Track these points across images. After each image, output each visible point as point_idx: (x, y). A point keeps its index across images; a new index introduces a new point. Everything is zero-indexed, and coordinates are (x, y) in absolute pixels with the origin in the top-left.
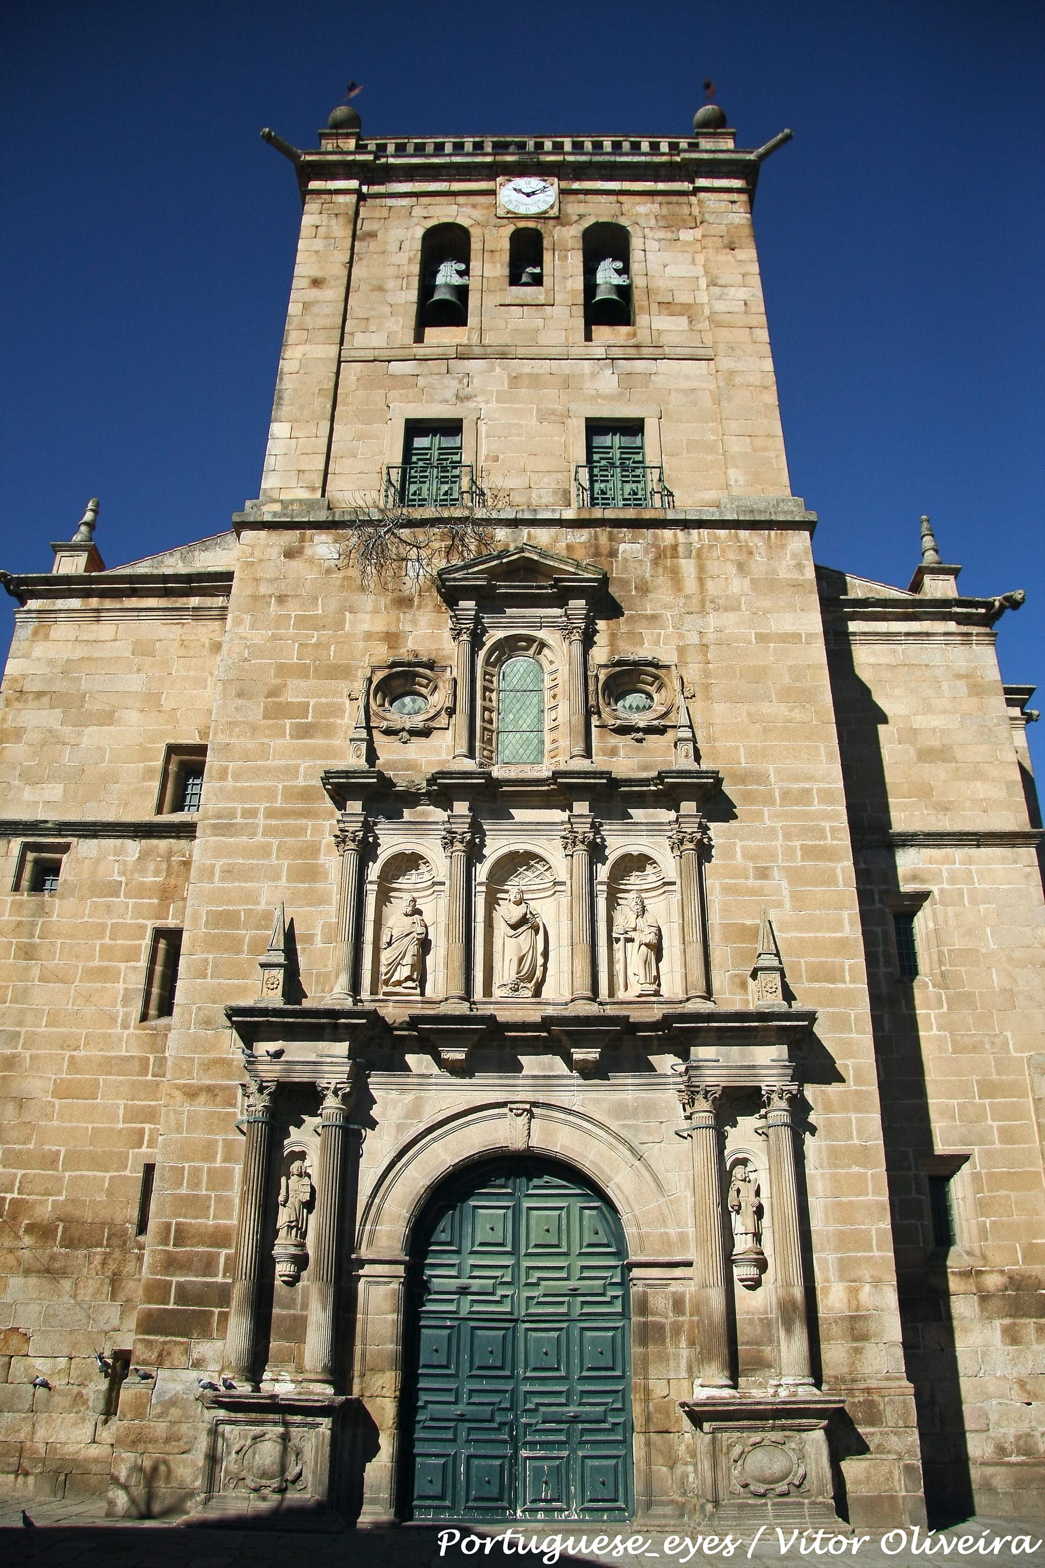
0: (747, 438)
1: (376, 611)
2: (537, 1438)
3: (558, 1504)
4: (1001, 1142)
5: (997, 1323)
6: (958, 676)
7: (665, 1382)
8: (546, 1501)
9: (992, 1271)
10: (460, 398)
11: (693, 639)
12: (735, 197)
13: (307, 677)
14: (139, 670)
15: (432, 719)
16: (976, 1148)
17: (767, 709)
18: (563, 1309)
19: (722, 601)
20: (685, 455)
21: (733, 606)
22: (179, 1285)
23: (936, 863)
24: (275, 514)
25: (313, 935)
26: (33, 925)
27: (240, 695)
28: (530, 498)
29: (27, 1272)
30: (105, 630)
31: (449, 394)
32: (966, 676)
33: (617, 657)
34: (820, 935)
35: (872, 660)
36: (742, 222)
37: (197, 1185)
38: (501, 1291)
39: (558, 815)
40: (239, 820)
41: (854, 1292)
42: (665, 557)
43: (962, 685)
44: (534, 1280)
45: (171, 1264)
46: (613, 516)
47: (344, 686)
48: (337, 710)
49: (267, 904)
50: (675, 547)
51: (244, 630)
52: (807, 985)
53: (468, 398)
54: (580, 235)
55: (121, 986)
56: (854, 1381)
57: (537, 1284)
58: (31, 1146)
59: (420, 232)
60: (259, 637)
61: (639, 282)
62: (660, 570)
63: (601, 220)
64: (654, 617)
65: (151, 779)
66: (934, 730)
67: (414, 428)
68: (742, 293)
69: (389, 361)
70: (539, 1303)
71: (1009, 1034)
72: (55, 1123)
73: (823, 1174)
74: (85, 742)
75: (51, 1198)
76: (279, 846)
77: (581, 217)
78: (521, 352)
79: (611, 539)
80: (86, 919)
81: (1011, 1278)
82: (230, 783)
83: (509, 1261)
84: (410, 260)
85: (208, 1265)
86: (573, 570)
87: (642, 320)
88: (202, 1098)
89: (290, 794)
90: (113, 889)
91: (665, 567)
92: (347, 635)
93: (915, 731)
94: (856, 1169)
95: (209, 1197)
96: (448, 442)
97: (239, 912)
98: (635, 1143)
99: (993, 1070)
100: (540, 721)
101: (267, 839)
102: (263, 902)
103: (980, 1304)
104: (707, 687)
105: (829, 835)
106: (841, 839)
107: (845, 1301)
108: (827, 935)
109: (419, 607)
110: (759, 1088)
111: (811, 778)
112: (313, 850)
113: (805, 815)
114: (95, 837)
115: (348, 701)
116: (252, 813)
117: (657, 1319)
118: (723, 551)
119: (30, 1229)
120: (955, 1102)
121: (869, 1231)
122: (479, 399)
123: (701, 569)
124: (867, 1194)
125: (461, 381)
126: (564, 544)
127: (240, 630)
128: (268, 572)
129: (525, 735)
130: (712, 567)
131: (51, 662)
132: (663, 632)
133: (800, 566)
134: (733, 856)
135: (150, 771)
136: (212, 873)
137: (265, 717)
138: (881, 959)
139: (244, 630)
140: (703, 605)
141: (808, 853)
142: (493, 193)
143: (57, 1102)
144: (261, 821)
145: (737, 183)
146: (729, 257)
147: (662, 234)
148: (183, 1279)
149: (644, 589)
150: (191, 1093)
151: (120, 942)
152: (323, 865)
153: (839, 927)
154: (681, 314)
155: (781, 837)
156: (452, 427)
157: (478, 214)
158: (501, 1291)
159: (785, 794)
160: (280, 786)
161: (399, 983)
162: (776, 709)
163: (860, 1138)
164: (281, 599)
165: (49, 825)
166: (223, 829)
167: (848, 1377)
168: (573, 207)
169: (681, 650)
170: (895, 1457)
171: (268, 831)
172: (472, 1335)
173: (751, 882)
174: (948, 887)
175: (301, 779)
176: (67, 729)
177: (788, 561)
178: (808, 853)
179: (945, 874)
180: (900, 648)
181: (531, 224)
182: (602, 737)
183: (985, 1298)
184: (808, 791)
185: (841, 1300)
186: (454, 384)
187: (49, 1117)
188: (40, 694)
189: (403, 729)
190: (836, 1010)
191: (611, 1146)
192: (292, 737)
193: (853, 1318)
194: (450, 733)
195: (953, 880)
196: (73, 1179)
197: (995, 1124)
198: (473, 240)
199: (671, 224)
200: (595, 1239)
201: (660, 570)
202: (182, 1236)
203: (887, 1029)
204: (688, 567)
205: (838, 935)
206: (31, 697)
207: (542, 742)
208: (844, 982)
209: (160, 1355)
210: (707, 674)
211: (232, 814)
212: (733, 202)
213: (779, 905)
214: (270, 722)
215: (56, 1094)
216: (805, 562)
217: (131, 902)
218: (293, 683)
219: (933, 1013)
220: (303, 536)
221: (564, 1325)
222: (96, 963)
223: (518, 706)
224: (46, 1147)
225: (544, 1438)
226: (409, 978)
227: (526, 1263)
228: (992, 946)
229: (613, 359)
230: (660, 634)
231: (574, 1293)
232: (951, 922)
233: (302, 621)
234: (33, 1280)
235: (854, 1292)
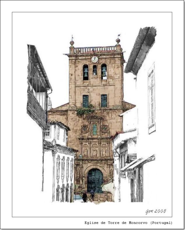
12: (119, 58)
59: (83, 65)
168: (101, 61)
204: (110, 114)
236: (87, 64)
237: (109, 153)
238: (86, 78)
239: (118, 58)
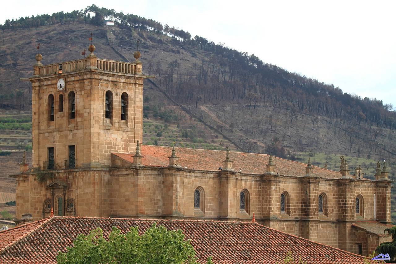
6: (132, 183)
11: (76, 194)
43: (132, 185)
59: (47, 97)
64: (72, 191)
87: (76, 118)
93: (125, 195)
130: (79, 179)
140: (78, 187)
142: (56, 84)
149: (72, 185)
164: (35, 188)
169: (75, 196)
186: (52, 138)
188: (20, 197)
204: (76, 180)
218: (37, 204)
238: (51, 118)
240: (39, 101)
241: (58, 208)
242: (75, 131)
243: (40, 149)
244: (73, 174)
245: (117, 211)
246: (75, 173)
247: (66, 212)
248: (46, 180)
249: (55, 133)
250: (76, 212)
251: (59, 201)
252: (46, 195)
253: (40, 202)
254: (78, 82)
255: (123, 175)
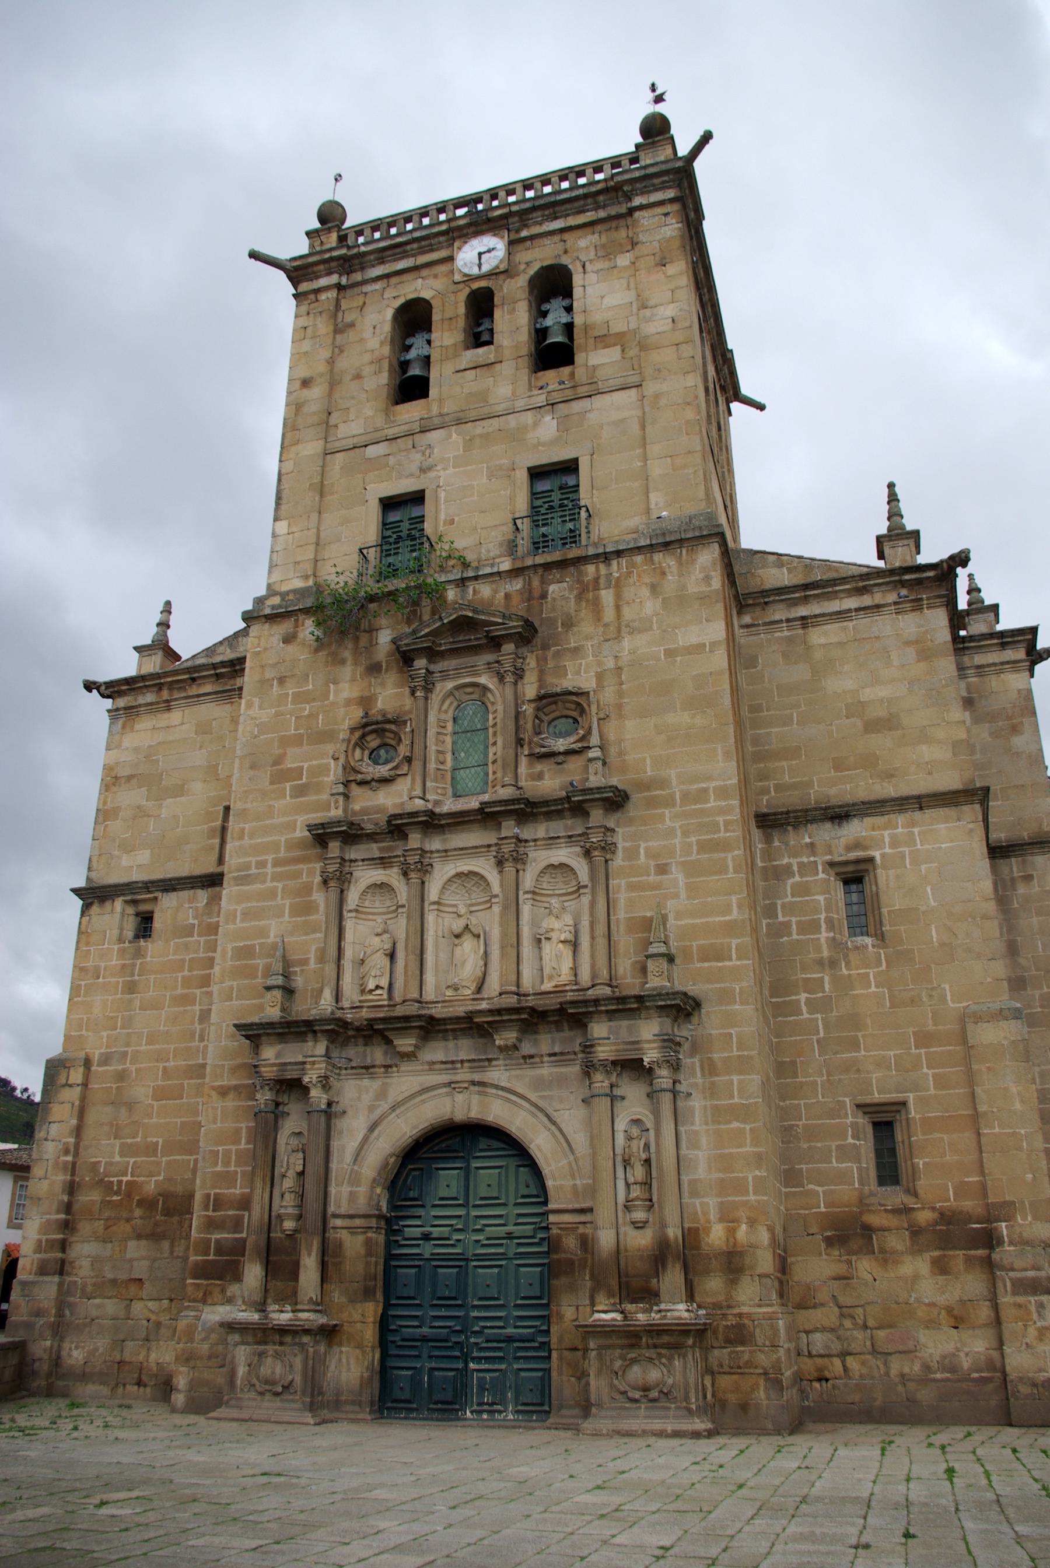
0: (669, 459)
1: (353, 680)
2: (482, 1354)
3: (499, 1407)
4: (935, 1088)
5: (928, 1255)
6: (908, 643)
7: (574, 1308)
8: (487, 1404)
9: (923, 1208)
10: (423, 470)
11: (610, 663)
12: (668, 208)
13: (301, 744)
14: (201, 747)
15: (395, 768)
16: (911, 1096)
17: (671, 719)
18: (501, 1250)
19: (636, 624)
20: (614, 487)
21: (644, 626)
22: (217, 1241)
23: (879, 828)
24: (273, 607)
25: (308, 959)
26: (134, 965)
27: (253, 767)
28: (480, 553)
29: (139, 1237)
30: (175, 716)
31: (414, 468)
32: (917, 642)
33: (542, 692)
34: (710, 919)
35: (823, 640)
36: (674, 234)
37: (227, 1163)
38: (455, 1237)
39: (490, 838)
40: (253, 871)
41: (731, 1232)
42: (588, 591)
43: (911, 652)
44: (478, 1227)
45: (211, 1225)
46: (542, 562)
47: (330, 748)
48: (324, 770)
49: (275, 937)
50: (596, 580)
51: (255, 711)
52: (698, 965)
53: (430, 469)
54: (526, 284)
55: (197, 1008)
56: (729, 1307)
57: (481, 1230)
58: (139, 1140)
59: (389, 314)
60: (265, 715)
61: (578, 320)
62: (584, 604)
63: (545, 264)
65: (213, 837)
66: (882, 701)
67: (389, 504)
68: (670, 311)
69: (366, 446)
70: (484, 1245)
71: (947, 987)
72: (155, 1120)
73: (707, 1131)
74: (164, 813)
75: (154, 1179)
76: (283, 889)
77: (528, 264)
78: (473, 414)
79: (543, 582)
80: (170, 957)
81: (942, 1214)
82: (246, 841)
83: (461, 1212)
84: (382, 343)
85: (237, 1225)
86: (500, 621)
87: (579, 358)
88: (231, 1095)
89: (291, 845)
90: (189, 931)
91: (587, 601)
92: (332, 704)
93: (863, 704)
94: (735, 1125)
95: (236, 1172)
96: (415, 512)
97: (254, 945)
98: (550, 1111)
99: (930, 1022)
100: (486, 755)
101: (275, 884)
102: (272, 935)
103: (911, 1238)
104: (620, 706)
105: (722, 828)
106: (733, 831)
107: (724, 1238)
108: (717, 919)
109: (387, 670)
110: (642, 1060)
111: (709, 778)
112: (307, 889)
113: (702, 812)
114: (174, 890)
115: (332, 761)
116: (262, 864)
117: (569, 1256)
118: (639, 576)
119: (140, 1203)
120: (892, 1053)
121: (746, 1179)
122: (438, 468)
123: (618, 596)
124: (746, 1146)
125: (424, 454)
126: (502, 594)
127: (251, 712)
128: (271, 658)
129: (473, 770)
130: (628, 593)
131: (136, 750)
132: (583, 662)
133: (707, 579)
134: (637, 857)
135: (212, 830)
136: (235, 917)
137: (272, 783)
138: (824, 926)
139: (255, 711)
140: (618, 631)
141: (704, 847)
142: (451, 259)
143: (155, 1103)
144: (269, 869)
145: (671, 194)
146: (661, 276)
147: (600, 265)
148: (218, 1236)
149: (569, 624)
150: (223, 1092)
151: (195, 973)
152: (315, 901)
153: (728, 910)
154: (614, 345)
155: (679, 833)
156: (417, 498)
157: (439, 284)
158: (455, 1237)
159: (685, 796)
160: (283, 840)
161: (371, 991)
162: (680, 718)
163: (741, 1097)
164: (282, 680)
165: (140, 885)
166: (243, 880)
167: (725, 1304)
168: (523, 256)
169: (600, 677)
170: (761, 1371)
171: (276, 877)
172: (517, 1272)
173: (652, 878)
174: (891, 851)
175: (298, 831)
176: (150, 803)
177: (697, 574)
178: (704, 847)
179: (887, 840)
180: (850, 624)
181: (483, 284)
182: (530, 765)
183: (915, 1232)
184: (705, 790)
185: (720, 1239)
187: (149, 1115)
188: (129, 778)
189: (373, 780)
190: (722, 985)
191: (534, 1115)
192: (291, 797)
193: (730, 1253)
194: (409, 777)
195: (894, 844)
196: (169, 1163)
197: (930, 1072)
198: (434, 311)
199: (608, 252)
200: (526, 1192)
201: (584, 604)
202: (219, 1203)
203: (827, 990)
204: (607, 596)
205: (727, 918)
206: (123, 780)
207: (487, 774)
208: (731, 960)
209: (205, 1294)
210: (620, 694)
211: (248, 866)
212: (666, 215)
213: (676, 896)
214: (275, 786)
215: (156, 1097)
216: (713, 574)
217: (202, 939)
218: (292, 751)
219: (871, 972)
220: (297, 621)
221: (503, 1263)
222: (179, 991)
223: (468, 745)
224: (149, 1140)
225: (487, 1354)
226: (377, 987)
227: (475, 1213)
228: (933, 903)
229: (553, 404)
230: (581, 664)
231: (510, 1236)
232: (892, 885)
233: (299, 698)
234: (143, 1242)
235: (731, 1232)
236: (426, 295)
237: (601, 942)
239: (659, 210)
240: (334, 338)
241: (449, 757)
242: (577, 406)
243: (325, 515)
244: (580, 574)
245: (809, 784)
246: (591, 569)
247: (523, 762)
248: (372, 630)
249: (434, 436)
250: (613, 750)
251: (455, 720)
252: (365, 701)
253: (324, 736)
254: (589, 230)
255: (840, 616)
